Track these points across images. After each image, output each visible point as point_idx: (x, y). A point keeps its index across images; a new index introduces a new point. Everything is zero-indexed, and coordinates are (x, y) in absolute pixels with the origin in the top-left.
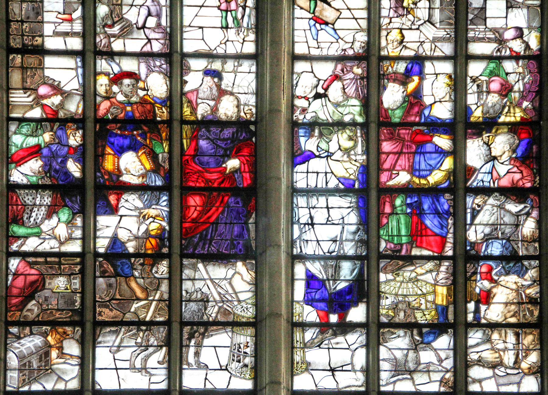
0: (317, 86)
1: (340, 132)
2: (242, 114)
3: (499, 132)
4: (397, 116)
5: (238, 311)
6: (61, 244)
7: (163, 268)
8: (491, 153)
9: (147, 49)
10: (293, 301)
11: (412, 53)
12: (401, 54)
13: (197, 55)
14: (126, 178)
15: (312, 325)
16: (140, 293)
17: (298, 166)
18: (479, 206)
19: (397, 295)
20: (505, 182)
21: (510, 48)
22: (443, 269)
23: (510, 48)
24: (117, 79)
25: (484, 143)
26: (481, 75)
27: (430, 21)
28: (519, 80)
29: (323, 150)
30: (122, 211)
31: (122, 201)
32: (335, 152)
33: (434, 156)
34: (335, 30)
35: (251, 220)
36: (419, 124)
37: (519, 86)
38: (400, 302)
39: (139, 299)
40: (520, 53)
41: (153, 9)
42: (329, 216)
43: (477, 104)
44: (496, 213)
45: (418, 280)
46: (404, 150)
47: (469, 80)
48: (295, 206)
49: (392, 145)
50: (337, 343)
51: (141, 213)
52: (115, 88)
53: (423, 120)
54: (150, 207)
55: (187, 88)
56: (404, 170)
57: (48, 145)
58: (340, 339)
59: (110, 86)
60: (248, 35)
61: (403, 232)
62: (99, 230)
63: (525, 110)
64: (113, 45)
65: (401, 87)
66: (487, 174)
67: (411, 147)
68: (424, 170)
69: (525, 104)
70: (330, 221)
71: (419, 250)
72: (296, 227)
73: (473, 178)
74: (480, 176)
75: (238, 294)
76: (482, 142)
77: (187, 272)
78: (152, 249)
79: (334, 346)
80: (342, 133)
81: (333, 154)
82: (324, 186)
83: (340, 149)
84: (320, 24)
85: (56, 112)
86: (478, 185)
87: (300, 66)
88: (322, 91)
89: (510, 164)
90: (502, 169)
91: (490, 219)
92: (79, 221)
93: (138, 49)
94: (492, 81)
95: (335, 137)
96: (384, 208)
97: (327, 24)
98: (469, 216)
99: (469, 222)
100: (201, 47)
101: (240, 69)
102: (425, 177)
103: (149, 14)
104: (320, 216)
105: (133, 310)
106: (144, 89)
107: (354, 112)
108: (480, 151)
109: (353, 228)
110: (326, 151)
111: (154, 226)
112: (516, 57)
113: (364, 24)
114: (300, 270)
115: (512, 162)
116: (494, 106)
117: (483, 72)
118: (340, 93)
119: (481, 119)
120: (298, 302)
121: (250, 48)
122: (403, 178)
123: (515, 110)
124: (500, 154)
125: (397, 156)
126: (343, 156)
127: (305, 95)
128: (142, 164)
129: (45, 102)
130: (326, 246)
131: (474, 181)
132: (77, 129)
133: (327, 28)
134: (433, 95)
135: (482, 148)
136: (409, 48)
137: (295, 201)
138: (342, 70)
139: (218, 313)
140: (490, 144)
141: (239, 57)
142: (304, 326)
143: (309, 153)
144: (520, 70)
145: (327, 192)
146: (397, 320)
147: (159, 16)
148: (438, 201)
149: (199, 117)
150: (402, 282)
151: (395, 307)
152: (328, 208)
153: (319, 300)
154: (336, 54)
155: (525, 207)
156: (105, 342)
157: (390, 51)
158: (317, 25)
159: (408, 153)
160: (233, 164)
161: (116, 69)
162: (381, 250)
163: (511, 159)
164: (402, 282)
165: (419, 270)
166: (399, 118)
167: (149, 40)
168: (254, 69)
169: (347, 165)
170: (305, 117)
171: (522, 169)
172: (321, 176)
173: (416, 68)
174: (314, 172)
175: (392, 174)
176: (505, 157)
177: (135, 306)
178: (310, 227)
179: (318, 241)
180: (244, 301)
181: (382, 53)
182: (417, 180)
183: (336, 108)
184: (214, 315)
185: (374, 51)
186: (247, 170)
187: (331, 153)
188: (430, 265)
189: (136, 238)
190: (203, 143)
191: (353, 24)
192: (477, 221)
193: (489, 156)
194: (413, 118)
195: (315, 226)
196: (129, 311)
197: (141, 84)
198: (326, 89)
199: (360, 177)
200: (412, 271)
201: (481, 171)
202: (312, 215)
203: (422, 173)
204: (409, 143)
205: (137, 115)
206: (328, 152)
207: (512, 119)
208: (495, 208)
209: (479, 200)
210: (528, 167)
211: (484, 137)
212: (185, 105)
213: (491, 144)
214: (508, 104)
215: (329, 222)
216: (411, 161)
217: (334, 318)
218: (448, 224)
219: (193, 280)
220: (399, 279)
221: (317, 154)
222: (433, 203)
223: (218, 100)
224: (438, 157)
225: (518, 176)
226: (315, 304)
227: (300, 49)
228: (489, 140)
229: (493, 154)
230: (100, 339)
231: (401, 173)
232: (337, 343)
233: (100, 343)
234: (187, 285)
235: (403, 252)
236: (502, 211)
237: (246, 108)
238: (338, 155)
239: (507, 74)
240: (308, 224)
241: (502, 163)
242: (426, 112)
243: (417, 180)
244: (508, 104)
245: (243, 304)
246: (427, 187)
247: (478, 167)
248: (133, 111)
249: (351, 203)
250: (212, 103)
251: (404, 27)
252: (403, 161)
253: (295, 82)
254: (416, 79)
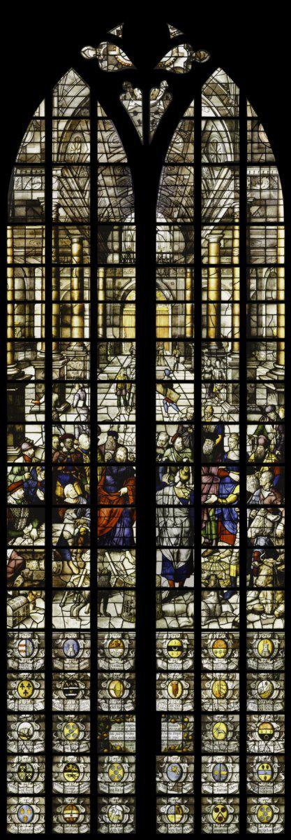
2: (129, 458)
5: (127, 581)
9: (78, 420)
11: (217, 420)
13: (104, 423)
15: (166, 589)
16: (76, 571)
19: (210, 571)
20: (266, 502)
24: (62, 439)
27: (227, 401)
30: (66, 521)
33: (230, 485)
34: (177, 406)
39: (75, 574)
41: (82, 395)
47: (247, 437)
51: (75, 522)
52: (62, 444)
58: (181, 597)
59: (60, 442)
60: (131, 410)
61: (213, 532)
63: (277, 456)
69: (277, 452)
74: (254, 498)
85: (31, 459)
93: (73, 420)
97: (173, 402)
100: (107, 418)
102: (225, 498)
103: (80, 399)
105: (71, 580)
106: (77, 444)
109: (187, 529)
111: (82, 529)
113: (192, 402)
116: (260, 453)
121: (133, 418)
122: (213, 499)
129: (25, 453)
133: (173, 405)
141: (126, 423)
144: (275, 431)
147: (84, 400)
150: (213, 563)
153: (169, 574)
160: (124, 490)
163: (270, 487)
164: (213, 563)
167: (79, 415)
176: (267, 487)
182: (220, 500)
190: (108, 478)
191: (186, 402)
207: (270, 461)
210: (279, 493)
215: (174, 525)
217: (177, 585)
219: (103, 562)
223: (116, 450)
225: (273, 498)
235: (214, 545)
236: (266, 520)
237: (131, 455)
243: (220, 500)
248: (71, 458)
250: (113, 452)
252: (213, 489)
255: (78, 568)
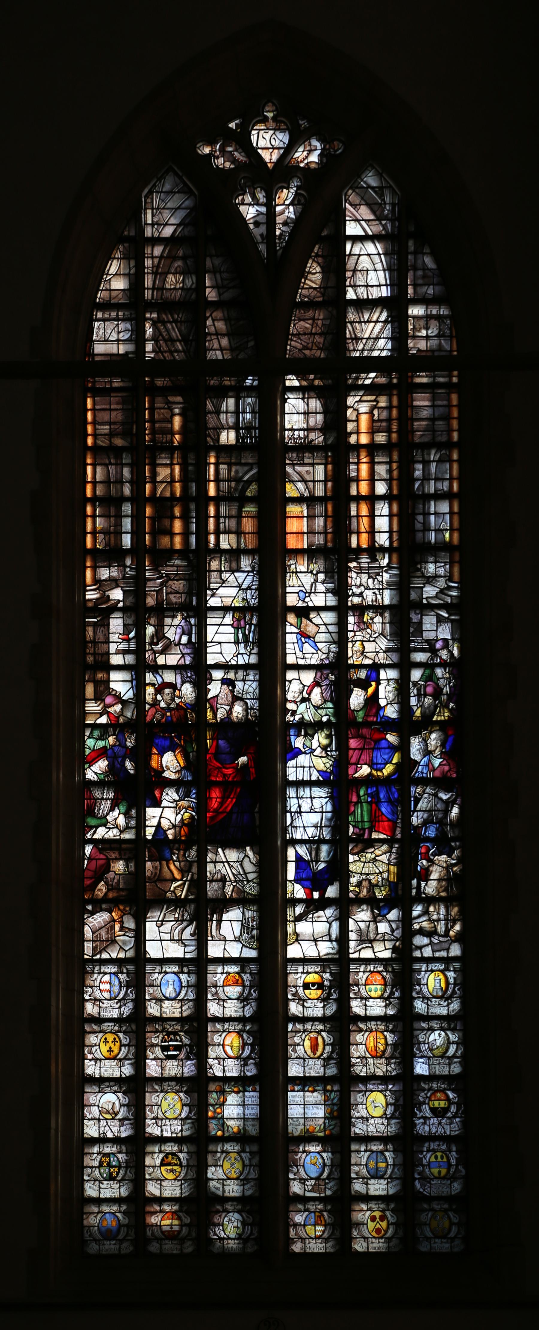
0: (302, 692)
4: (360, 717)
5: (247, 889)
6: (121, 832)
7: (193, 853)
9: (182, 662)
10: (287, 880)
11: (370, 662)
13: (217, 666)
14: (166, 774)
15: (300, 901)
16: (177, 875)
18: (419, 794)
19: (361, 874)
22: (394, 850)
27: (382, 634)
30: (164, 803)
31: (164, 794)
33: (387, 751)
34: (315, 643)
35: (256, 810)
36: (376, 723)
37: (446, 690)
38: (363, 879)
39: (177, 880)
45: (376, 860)
50: (319, 917)
51: (177, 805)
52: (159, 697)
54: (184, 800)
55: (209, 696)
56: (365, 764)
57: (113, 746)
58: (321, 913)
60: (253, 649)
62: (149, 819)
64: (157, 660)
67: (371, 744)
71: (377, 834)
72: (288, 815)
75: (248, 875)
77: (210, 856)
78: (186, 836)
79: (317, 919)
81: (315, 750)
83: (319, 746)
84: (305, 638)
87: (290, 675)
88: (307, 696)
90: (437, 762)
92: (133, 812)
95: (316, 736)
101: (248, 678)
102: (381, 770)
104: (306, 806)
106: (179, 697)
109: (329, 815)
111: (187, 816)
112: (443, 664)
114: (291, 854)
116: (429, 706)
118: (319, 697)
120: (290, 881)
122: (365, 770)
128: (178, 762)
130: (311, 832)
131: (416, 773)
132: (132, 733)
133: (310, 642)
138: (321, 677)
139: (233, 891)
142: (295, 902)
144: (447, 675)
145: (310, 784)
146: (361, 896)
149: (219, 720)
150: (365, 862)
151: (359, 884)
152: (311, 798)
156: (152, 917)
158: (303, 639)
159: (369, 749)
160: (243, 759)
161: (160, 680)
162: (350, 834)
164: (365, 862)
165: (377, 852)
168: (257, 677)
169: (324, 760)
172: (306, 769)
177: (174, 885)
179: (304, 827)
180: (252, 881)
181: (349, 662)
182: (374, 772)
184: (230, 893)
186: (253, 765)
188: (385, 847)
189: (174, 826)
196: (169, 890)
197: (177, 693)
198: (309, 694)
200: (372, 853)
205: (175, 719)
212: (209, 710)
215: (312, 811)
217: (316, 895)
219: (215, 862)
220: (363, 859)
221: (303, 751)
223: (232, 706)
226: (303, 882)
227: (290, 660)
230: (148, 915)
232: (319, 917)
233: (149, 918)
234: (210, 867)
235: (366, 836)
238: (318, 752)
240: (297, 812)
241: (436, 757)
242: (381, 713)
243: (374, 772)
245: (251, 883)
251: (365, 639)
255: (181, 870)
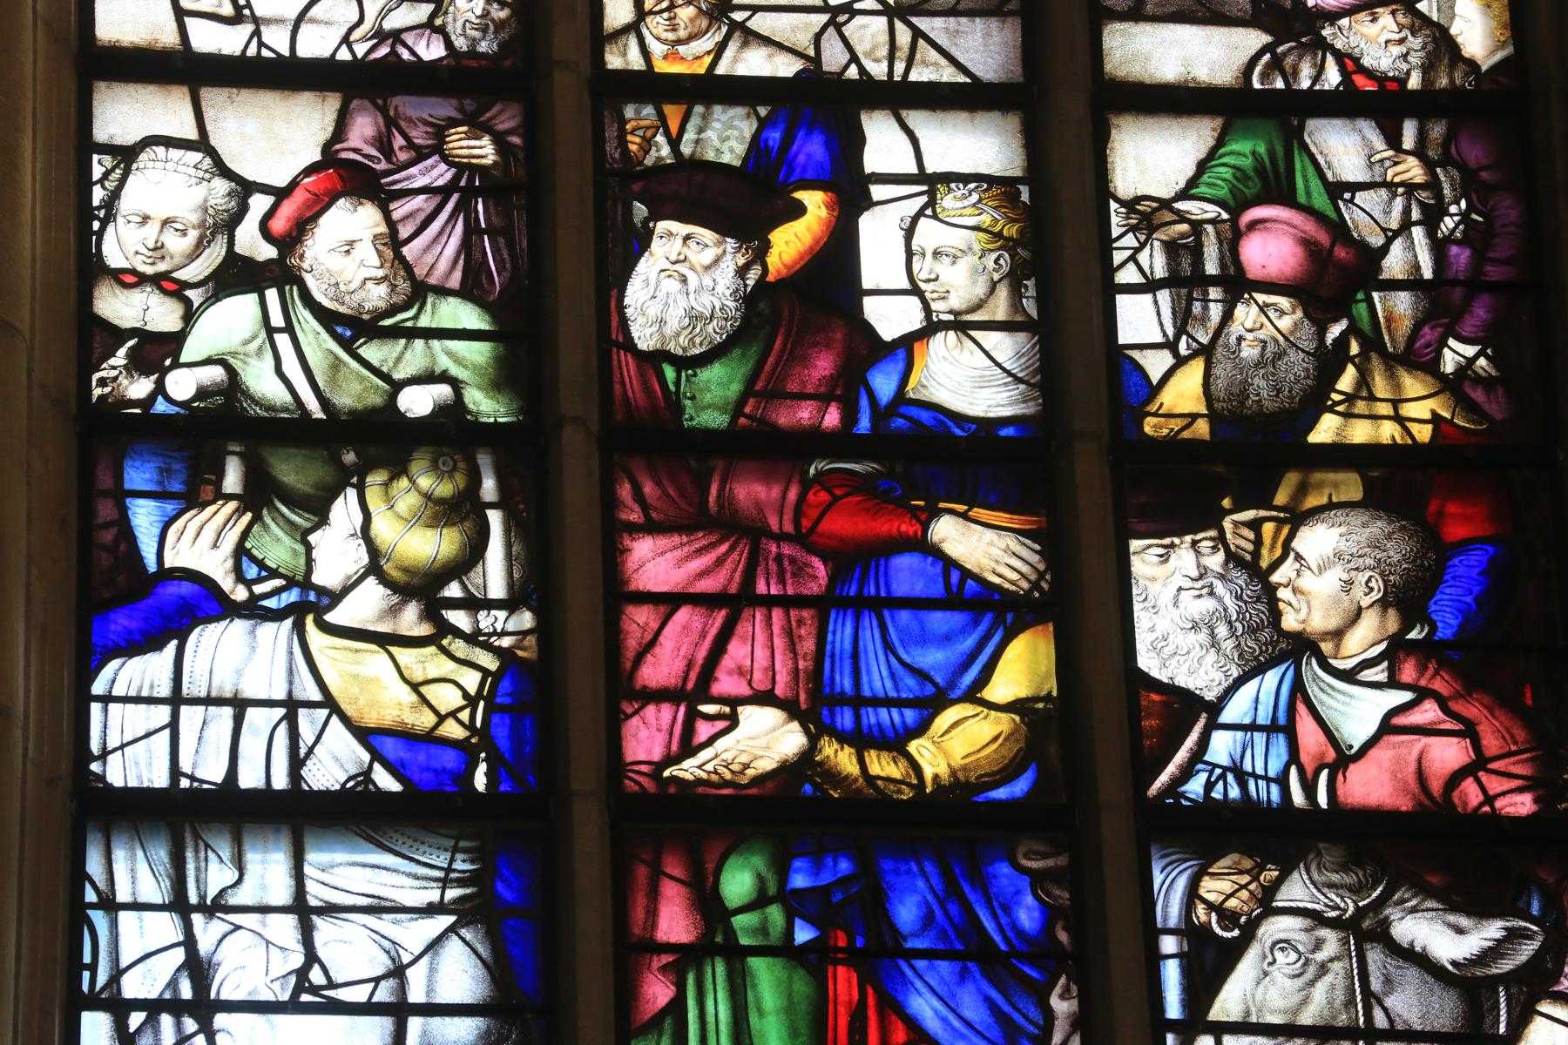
1: (375, 479)
3: (1312, 501)
8: (1276, 615)
11: (786, 67)
12: (721, 70)
17: (114, 664)
18: (1228, 918)
21: (1340, 57)
23: (1340, 57)
25: (1232, 558)
26: (1183, 195)
28: (1406, 225)
29: (274, 573)
32: (347, 589)
33: (939, 621)
36: (842, 443)
40: (1402, 81)
42: (312, 957)
43: (1171, 346)
44: (1337, 966)
46: (761, 588)
48: (90, 896)
49: (688, 558)
53: (864, 424)
56: (764, 698)
63: (1453, 386)
65: (731, 243)
66: (1259, 738)
67: (800, 570)
68: (888, 702)
70: (315, 990)
73: (1182, 755)
74: (1222, 747)
76: (1220, 556)
80: (386, 485)
81: (335, 597)
82: (280, 782)
83: (375, 568)
86: (1217, 794)
88: (267, 252)
89: (1393, 683)
91: (1305, 1002)
94: (1254, 225)
95: (345, 510)
96: (652, 914)
98: (1171, 973)
99: (1173, 1010)
102: (895, 743)
107: (456, 371)
108: (1209, 604)
110: (291, 583)
115: (1408, 673)
116: (1271, 359)
117: (1192, 182)
119: (1202, 428)
123: (1397, 387)
124: (1333, 623)
125: (720, 617)
126: (394, 611)
127: (162, 267)
131: (1187, 773)
134: (915, 291)
135: (1220, 588)
136: (767, 41)
137: (94, 866)
138: (383, 144)
140: (1264, 564)
143: (186, 588)
144: (1413, 170)
148: (984, 886)
152: (302, 910)
154: (344, 55)
155: (1513, 936)
157: (657, 49)
159: (785, 602)
163: (1395, 650)
166: (722, 409)
170: (160, 388)
171: (1471, 710)
172: (259, 721)
173: (812, 149)
174: (220, 702)
175: (693, 717)
176: (1363, 639)
178: (190, 1025)
181: (614, 61)
182: (844, 759)
183: (347, 345)
185: (565, 41)
187: (322, 591)
192: (1228, 1003)
193: (1265, 635)
194: (804, 414)
195: (221, 1020)
198: (290, 241)
199: (501, 732)
201: (1227, 716)
202: (204, 946)
203: (871, 717)
204: (787, 550)
206: (306, 584)
207: (1388, 432)
208: (1331, 937)
209: (1226, 886)
210: (1504, 700)
211: (1227, 524)
213: (1275, 566)
214: (1355, 349)
216: (809, 645)
218: (1049, 1015)
221: (241, 594)
222: (950, 892)
224: (963, 632)
225: (1448, 754)
228: (1258, 542)
229: (1290, 622)
231: (747, 713)
236: (1375, 956)
239: (1339, 190)
240: (176, 1007)
241: (1349, 676)
242: (884, 383)
243: (844, 759)
244: (1355, 349)
246: (907, 794)
247: (1210, 696)
249: (445, 883)
253: (98, 195)
254: (815, 202)
